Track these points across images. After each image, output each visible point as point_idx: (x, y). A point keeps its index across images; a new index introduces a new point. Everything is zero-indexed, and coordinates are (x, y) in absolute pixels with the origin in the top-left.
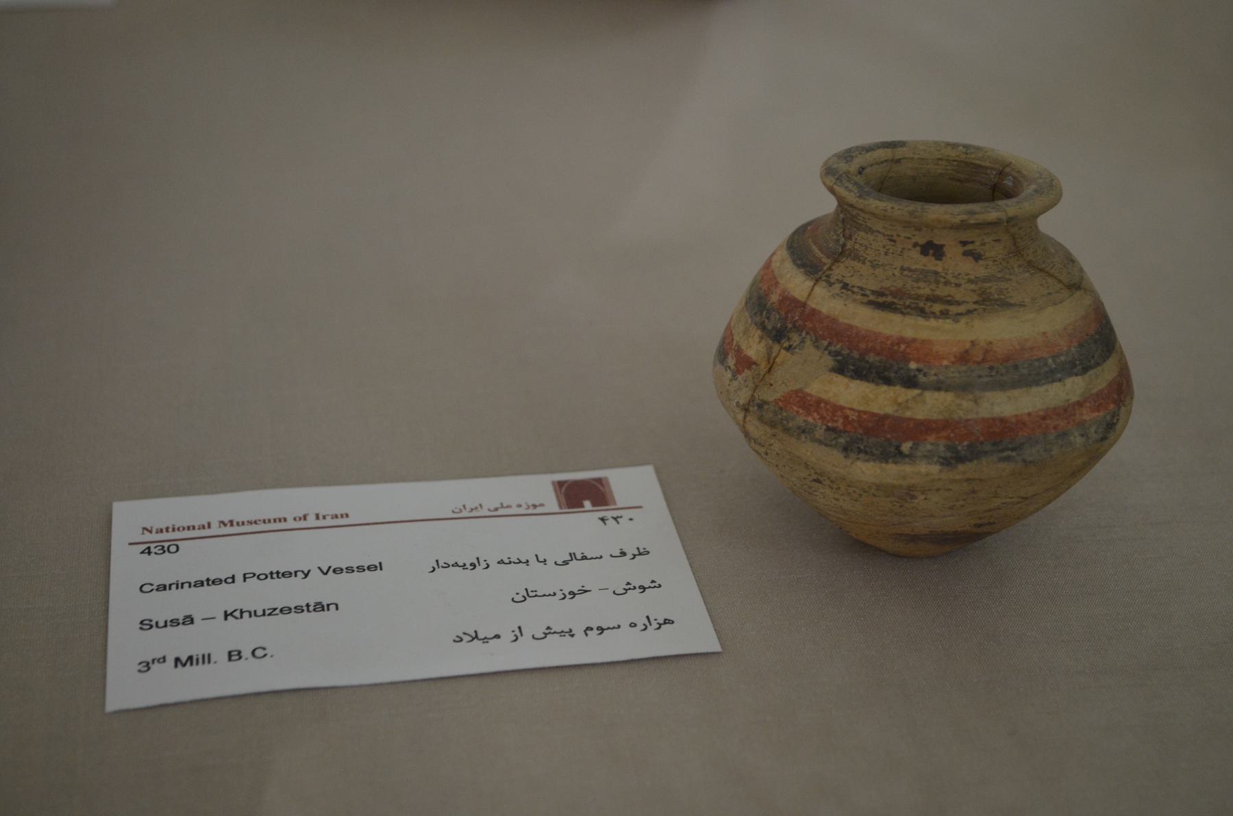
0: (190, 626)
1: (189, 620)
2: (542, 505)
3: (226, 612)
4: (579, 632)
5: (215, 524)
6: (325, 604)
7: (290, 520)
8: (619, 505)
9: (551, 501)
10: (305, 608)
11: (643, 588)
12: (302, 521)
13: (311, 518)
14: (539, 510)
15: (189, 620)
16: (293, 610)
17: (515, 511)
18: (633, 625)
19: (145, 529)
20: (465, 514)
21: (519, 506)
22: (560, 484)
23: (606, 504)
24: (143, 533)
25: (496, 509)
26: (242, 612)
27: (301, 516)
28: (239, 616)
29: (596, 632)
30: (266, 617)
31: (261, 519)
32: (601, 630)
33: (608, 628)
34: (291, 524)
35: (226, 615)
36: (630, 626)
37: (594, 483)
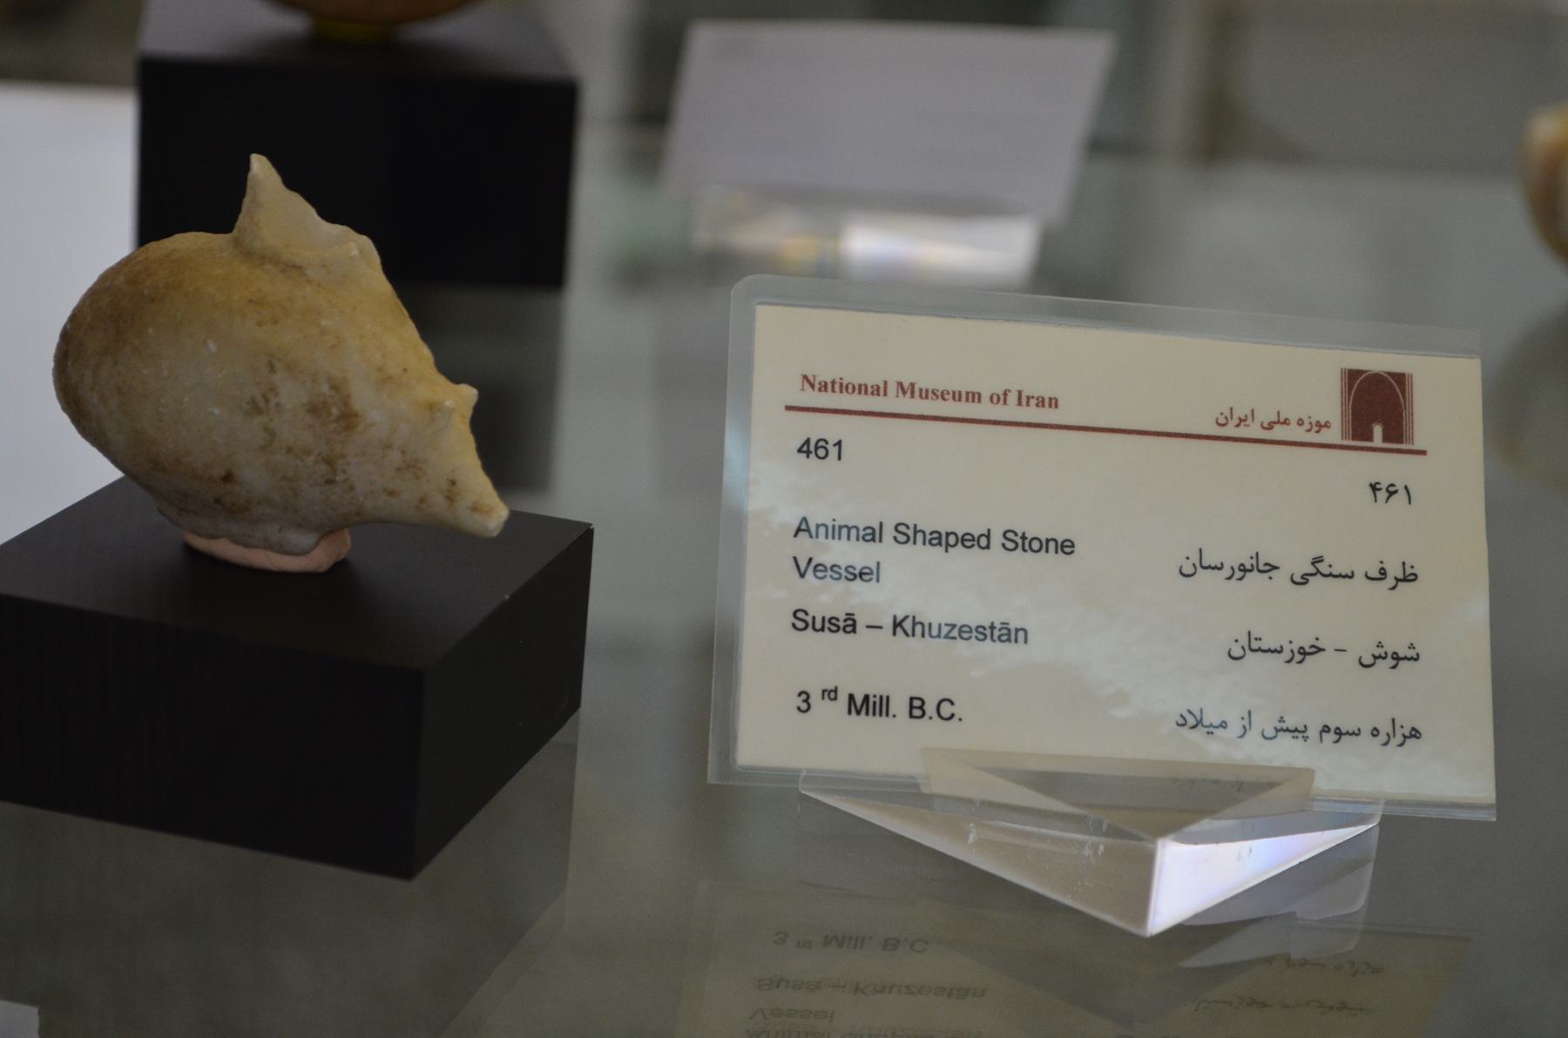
0: (852, 634)
1: (850, 625)
3: (895, 617)
4: (1313, 732)
5: (892, 389)
6: (1012, 627)
8: (1417, 446)
10: (988, 632)
13: (1012, 398)
15: (850, 625)
16: (974, 634)
18: (1375, 732)
19: (805, 377)
23: (1401, 442)
24: (803, 389)
26: (914, 624)
27: (1001, 392)
28: (910, 632)
29: (1331, 736)
30: (942, 641)
31: (950, 389)
33: (1348, 733)
34: (985, 410)
35: (897, 625)
36: (1375, 729)
37: (1386, 375)
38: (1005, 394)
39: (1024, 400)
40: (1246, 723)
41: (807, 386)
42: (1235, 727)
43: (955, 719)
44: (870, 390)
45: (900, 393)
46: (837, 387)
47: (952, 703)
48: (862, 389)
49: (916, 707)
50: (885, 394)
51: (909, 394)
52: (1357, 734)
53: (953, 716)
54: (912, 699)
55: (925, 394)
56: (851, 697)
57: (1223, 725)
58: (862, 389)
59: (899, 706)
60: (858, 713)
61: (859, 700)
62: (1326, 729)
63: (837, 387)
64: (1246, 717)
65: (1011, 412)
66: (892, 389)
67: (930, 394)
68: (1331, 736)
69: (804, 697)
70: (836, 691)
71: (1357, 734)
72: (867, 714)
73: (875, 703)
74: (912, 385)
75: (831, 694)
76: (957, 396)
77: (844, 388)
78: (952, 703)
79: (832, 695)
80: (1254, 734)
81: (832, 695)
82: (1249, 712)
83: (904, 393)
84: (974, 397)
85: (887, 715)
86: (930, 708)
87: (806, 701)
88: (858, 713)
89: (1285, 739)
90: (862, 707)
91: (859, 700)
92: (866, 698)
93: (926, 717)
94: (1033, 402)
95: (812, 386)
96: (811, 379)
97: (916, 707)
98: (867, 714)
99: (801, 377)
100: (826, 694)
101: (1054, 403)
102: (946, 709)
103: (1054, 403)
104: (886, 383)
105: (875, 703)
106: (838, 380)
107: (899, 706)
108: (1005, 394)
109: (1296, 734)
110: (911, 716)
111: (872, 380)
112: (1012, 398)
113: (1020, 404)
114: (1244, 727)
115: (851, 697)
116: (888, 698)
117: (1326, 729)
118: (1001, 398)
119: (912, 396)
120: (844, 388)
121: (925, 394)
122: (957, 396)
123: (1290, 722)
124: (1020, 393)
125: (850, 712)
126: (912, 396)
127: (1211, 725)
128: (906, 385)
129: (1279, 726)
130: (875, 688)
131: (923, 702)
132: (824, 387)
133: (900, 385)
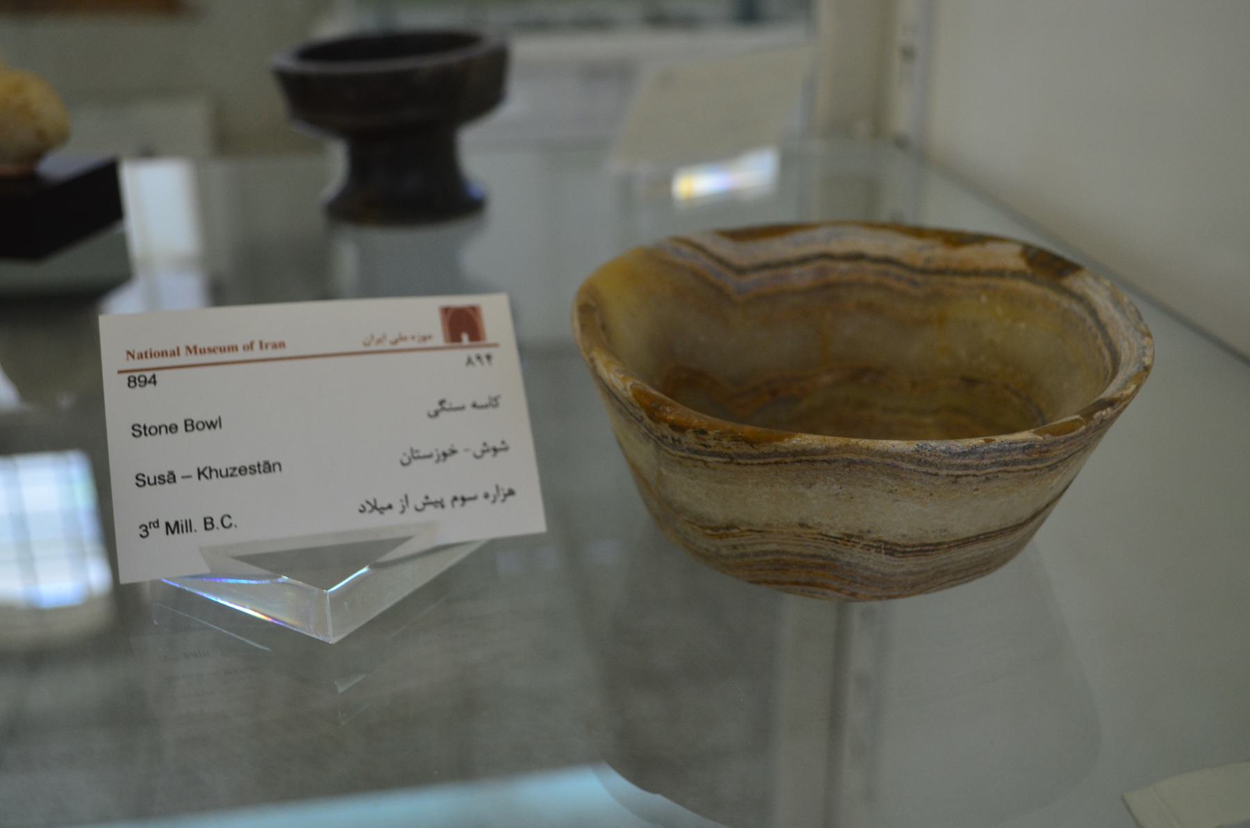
2: (430, 337)
4: (447, 502)
5: (183, 351)
7: (240, 348)
9: (436, 330)
11: (495, 450)
12: (250, 351)
13: (256, 346)
14: (429, 344)
17: (410, 344)
19: (129, 353)
20: (373, 347)
21: (413, 338)
22: (445, 311)
24: (128, 359)
25: (395, 342)
32: (464, 499)
34: (241, 355)
38: (252, 344)
39: (264, 346)
40: (404, 503)
41: (130, 357)
42: (397, 507)
43: (233, 526)
44: (169, 353)
45: (188, 352)
46: (149, 355)
47: (229, 517)
48: (164, 354)
49: (208, 523)
50: (178, 354)
51: (193, 352)
52: (474, 498)
53: (231, 525)
54: (205, 519)
55: (203, 351)
56: (168, 524)
57: (390, 507)
58: (164, 354)
59: (198, 524)
60: (173, 532)
61: (172, 525)
62: (455, 499)
63: (149, 355)
64: (403, 498)
65: (257, 353)
66: (183, 351)
67: (207, 351)
68: (458, 503)
69: (144, 528)
70: (158, 522)
71: (474, 498)
72: (178, 532)
73: (182, 526)
74: (195, 348)
75: (156, 524)
76: (222, 350)
77: (153, 355)
78: (229, 517)
79: (156, 525)
80: (410, 510)
81: (156, 525)
82: (406, 497)
83: (191, 352)
84: (234, 348)
85: (191, 530)
86: (217, 523)
87: (146, 531)
88: (173, 532)
89: (430, 508)
90: (174, 528)
91: (172, 525)
92: (177, 523)
93: (215, 528)
94: (270, 347)
95: (133, 357)
96: (132, 352)
97: (208, 523)
98: (178, 532)
99: (125, 354)
100: (152, 525)
101: (282, 345)
102: (227, 522)
103: (282, 345)
104: (178, 349)
105: (182, 526)
106: (148, 350)
107: (198, 524)
108: (252, 344)
109: (436, 504)
110: (206, 529)
111: (169, 347)
112: (256, 346)
113: (261, 347)
114: (404, 507)
115: (168, 524)
116: (190, 521)
117: (455, 499)
118: (250, 346)
119: (196, 352)
120: (153, 355)
121: (203, 351)
122: (222, 350)
123: (432, 499)
124: (261, 343)
125: (167, 533)
126: (196, 352)
127: (383, 508)
128: (191, 347)
129: (425, 501)
130: (181, 518)
131: (212, 519)
132: (141, 356)
133: (188, 348)
